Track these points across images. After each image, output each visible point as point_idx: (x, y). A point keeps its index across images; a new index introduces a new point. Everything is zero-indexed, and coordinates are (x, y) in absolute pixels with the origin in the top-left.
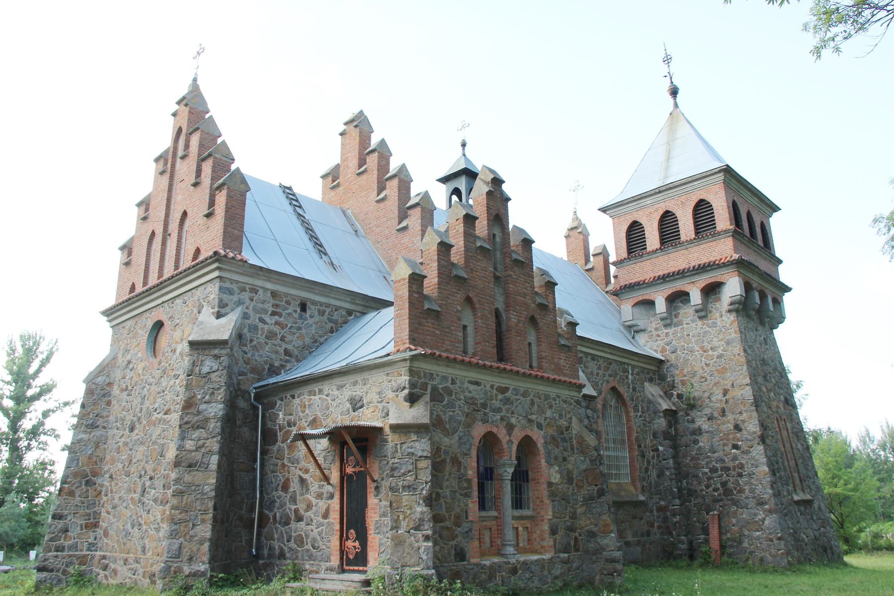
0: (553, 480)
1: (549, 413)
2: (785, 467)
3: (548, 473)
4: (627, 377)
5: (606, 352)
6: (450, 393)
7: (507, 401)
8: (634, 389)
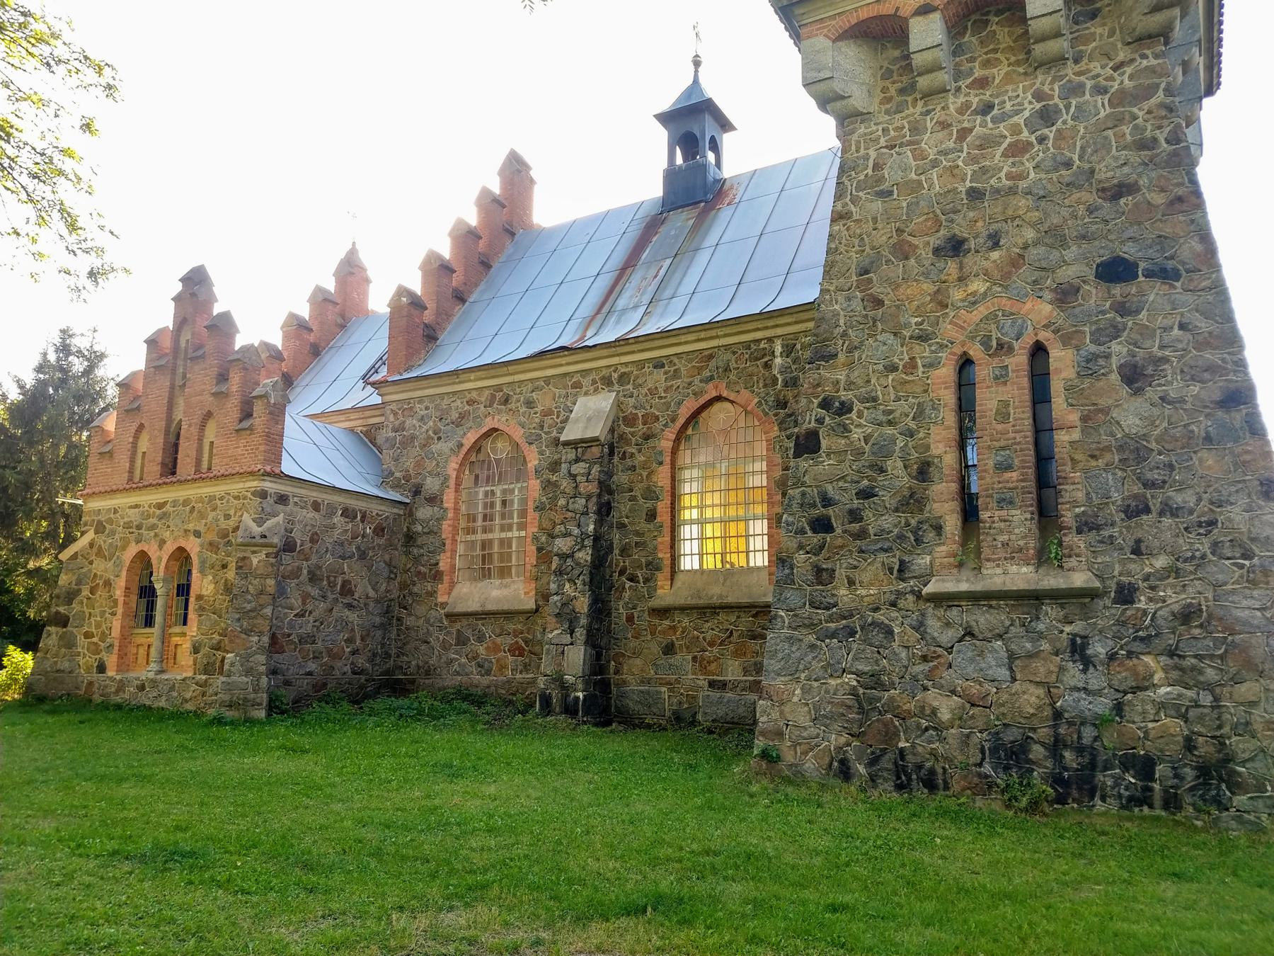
0: (204, 592)
1: (211, 515)
2: (912, 502)
3: (203, 585)
4: (767, 366)
5: (686, 343)
6: (110, 521)
7: (164, 516)
8: (792, 383)
